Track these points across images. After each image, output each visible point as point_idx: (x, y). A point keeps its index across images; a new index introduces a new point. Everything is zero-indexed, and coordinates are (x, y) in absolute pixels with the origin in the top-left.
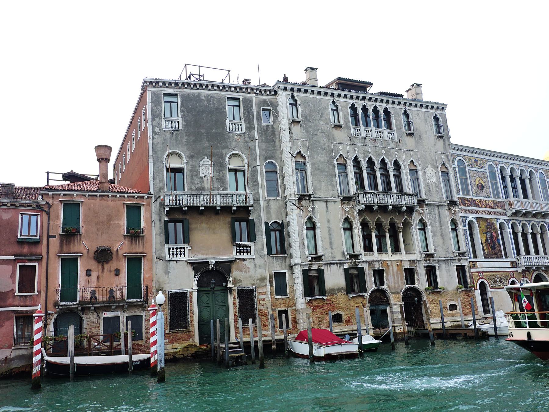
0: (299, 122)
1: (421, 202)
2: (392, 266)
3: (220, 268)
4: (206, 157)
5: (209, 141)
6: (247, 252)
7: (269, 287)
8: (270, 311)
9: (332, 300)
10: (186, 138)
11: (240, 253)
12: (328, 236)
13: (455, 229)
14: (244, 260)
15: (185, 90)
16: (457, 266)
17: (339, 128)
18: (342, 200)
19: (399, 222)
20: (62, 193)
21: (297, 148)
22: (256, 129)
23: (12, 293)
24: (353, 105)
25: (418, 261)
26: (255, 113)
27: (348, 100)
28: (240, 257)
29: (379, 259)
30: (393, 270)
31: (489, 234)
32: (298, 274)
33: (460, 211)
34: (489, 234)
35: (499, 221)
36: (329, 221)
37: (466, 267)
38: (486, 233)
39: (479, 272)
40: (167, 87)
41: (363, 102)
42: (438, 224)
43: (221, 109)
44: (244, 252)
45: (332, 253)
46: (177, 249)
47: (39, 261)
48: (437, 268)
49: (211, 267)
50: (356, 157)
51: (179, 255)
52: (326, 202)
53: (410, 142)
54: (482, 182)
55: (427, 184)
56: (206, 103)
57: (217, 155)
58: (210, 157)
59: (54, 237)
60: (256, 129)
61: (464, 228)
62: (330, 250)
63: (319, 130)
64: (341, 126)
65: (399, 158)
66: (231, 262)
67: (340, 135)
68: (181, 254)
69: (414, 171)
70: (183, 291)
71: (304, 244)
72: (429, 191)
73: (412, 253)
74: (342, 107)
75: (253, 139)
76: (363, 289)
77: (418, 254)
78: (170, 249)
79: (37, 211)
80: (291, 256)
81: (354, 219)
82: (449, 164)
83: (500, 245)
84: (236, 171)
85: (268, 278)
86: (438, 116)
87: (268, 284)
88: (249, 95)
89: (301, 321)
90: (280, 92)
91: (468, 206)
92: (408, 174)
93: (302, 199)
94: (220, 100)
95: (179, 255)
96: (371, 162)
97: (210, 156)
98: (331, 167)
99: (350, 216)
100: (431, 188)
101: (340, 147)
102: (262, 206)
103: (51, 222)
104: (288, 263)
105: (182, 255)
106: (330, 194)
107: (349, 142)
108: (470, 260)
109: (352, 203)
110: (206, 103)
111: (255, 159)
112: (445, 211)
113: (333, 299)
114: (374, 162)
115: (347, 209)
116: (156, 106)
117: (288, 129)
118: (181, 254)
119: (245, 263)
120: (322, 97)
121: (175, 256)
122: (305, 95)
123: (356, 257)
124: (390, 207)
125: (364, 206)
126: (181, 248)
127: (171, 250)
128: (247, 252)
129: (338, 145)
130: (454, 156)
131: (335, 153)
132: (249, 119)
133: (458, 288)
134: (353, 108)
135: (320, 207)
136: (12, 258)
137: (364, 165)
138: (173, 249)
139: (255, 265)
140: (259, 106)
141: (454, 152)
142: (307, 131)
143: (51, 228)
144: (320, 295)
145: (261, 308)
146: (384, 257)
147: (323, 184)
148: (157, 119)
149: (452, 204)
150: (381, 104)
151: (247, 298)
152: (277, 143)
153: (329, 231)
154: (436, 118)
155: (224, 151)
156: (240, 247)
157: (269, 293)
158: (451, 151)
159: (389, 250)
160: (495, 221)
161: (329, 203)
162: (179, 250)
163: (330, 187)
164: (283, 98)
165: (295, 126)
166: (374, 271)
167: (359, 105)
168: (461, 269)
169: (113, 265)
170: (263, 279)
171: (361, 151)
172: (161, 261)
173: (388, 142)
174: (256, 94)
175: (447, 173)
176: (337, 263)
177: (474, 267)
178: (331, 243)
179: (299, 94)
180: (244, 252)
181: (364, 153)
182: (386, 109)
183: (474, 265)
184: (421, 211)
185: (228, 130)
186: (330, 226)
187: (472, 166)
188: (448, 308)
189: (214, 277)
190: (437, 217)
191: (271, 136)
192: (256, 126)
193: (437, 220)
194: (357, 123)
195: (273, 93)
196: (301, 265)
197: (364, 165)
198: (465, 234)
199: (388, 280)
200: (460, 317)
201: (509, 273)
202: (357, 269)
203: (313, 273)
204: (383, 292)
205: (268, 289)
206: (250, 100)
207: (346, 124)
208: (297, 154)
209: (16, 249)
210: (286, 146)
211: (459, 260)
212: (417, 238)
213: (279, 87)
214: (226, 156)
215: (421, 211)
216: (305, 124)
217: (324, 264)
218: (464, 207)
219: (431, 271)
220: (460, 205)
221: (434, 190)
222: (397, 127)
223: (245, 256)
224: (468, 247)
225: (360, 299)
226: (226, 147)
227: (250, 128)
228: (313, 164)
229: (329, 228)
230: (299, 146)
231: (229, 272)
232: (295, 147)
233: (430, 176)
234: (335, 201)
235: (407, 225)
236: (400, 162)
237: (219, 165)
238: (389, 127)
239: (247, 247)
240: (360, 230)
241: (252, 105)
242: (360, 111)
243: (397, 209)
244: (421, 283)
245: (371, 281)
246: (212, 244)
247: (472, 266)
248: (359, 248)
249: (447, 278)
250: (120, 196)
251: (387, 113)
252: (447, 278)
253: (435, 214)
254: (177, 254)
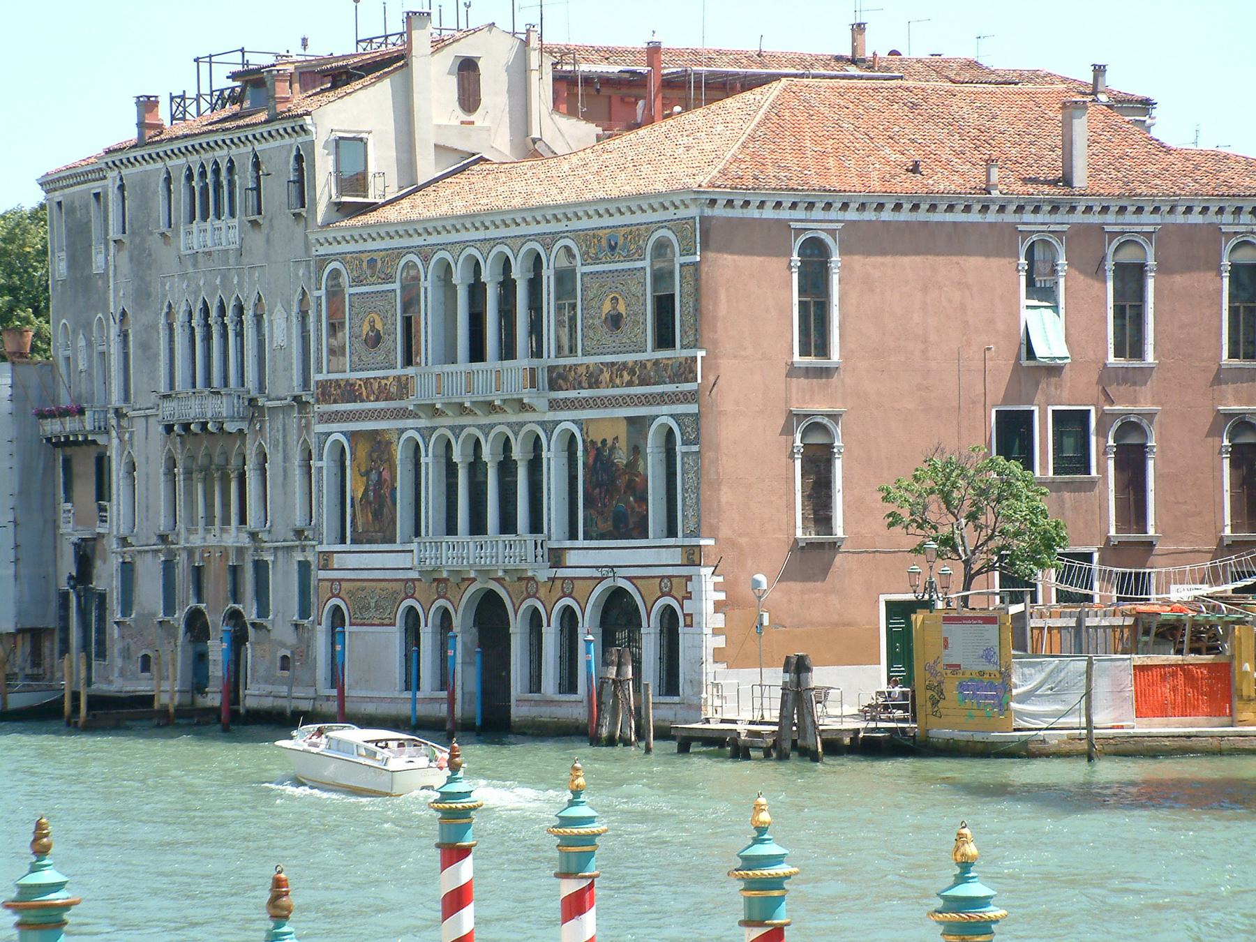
31: (374, 476)
34: (374, 476)
35: (405, 436)
38: (367, 473)
39: (332, 581)
42: (280, 455)
54: (379, 326)
66: (94, 539)
83: (395, 504)
91: (335, 402)
131: (162, 303)
135: (139, 426)
160: (394, 438)
183: (326, 560)
187: (358, 281)
188: (279, 664)
194: (193, 218)
200: (285, 689)
201: (402, 584)
211: (303, 549)
218: (325, 408)
220: (318, 401)
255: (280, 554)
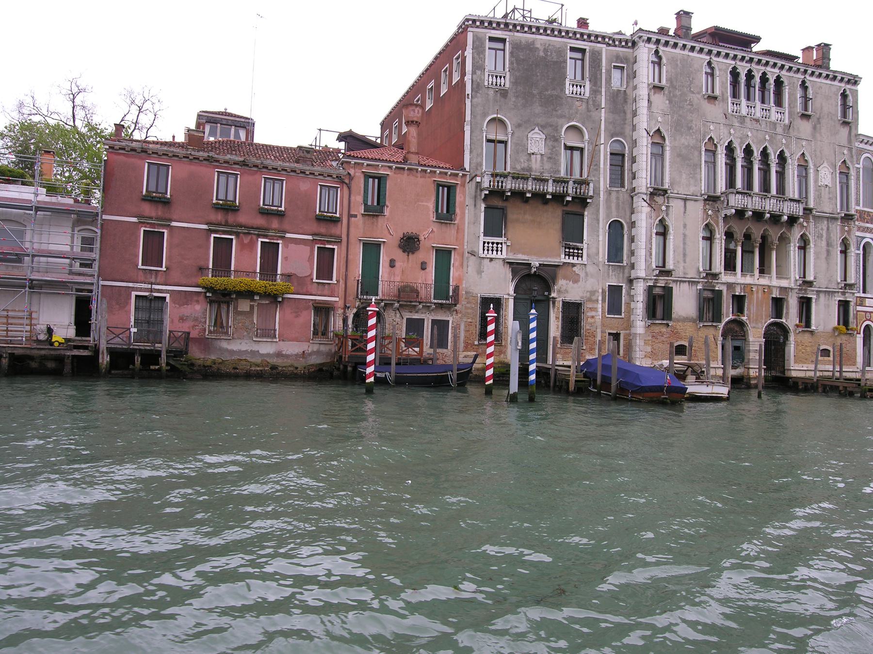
0: (662, 88)
1: (808, 211)
2: (757, 292)
3: (543, 274)
4: (537, 130)
5: (541, 106)
6: (578, 256)
7: (600, 302)
8: (599, 330)
9: (678, 327)
10: (513, 99)
11: (569, 256)
12: (682, 245)
13: (844, 252)
14: (573, 265)
15: (516, 34)
16: (839, 301)
17: (712, 101)
18: (705, 200)
19: (774, 234)
20: (366, 163)
21: (655, 124)
22: (603, 93)
23: (309, 279)
24: (735, 68)
25: (792, 289)
26: (604, 71)
27: (729, 61)
28: (568, 261)
29: (742, 282)
30: (757, 297)
32: (640, 290)
33: (856, 229)
36: (685, 226)
37: (852, 304)
39: (866, 312)
40: (494, 29)
41: (748, 65)
42: (824, 243)
43: (561, 62)
44: (573, 256)
45: (684, 268)
46: (493, 243)
47: (339, 242)
48: (814, 301)
49: (534, 270)
50: (730, 143)
51: (495, 252)
52: (685, 200)
53: (805, 127)
55: (818, 188)
56: (542, 54)
57: (551, 126)
58: (542, 127)
59: (356, 216)
60: (603, 93)
61: (858, 252)
62: (682, 264)
63: (686, 101)
64: (715, 98)
65: (787, 147)
67: (713, 111)
68: (497, 251)
69: (803, 167)
70: (497, 296)
71: (651, 254)
72: (819, 197)
73: (783, 279)
74: (720, 70)
75: (598, 107)
76: (717, 317)
77: (793, 279)
78: (484, 243)
79: (337, 182)
80: (632, 266)
81: (718, 226)
82: (852, 162)
84: (572, 149)
85: (600, 291)
86: (848, 92)
87: (600, 298)
88: (599, 45)
89: (638, 349)
90: (641, 44)
92: (796, 172)
93: (655, 194)
94: (560, 52)
95: (495, 252)
96: (748, 151)
97: (542, 126)
98: (696, 153)
99: (712, 222)
100: (823, 194)
101: (712, 127)
102: (601, 199)
103: (352, 198)
104: (626, 275)
105: (499, 253)
106: (692, 189)
107: (723, 121)
108: (858, 295)
109: (718, 205)
110: (542, 54)
111: (599, 135)
112: (836, 227)
113: (679, 326)
114: (752, 151)
115: (710, 212)
116: (478, 54)
117: (646, 97)
118: (497, 251)
119: (575, 269)
120: (695, 54)
121: (490, 252)
122: (673, 50)
123: (715, 276)
124: (768, 215)
125: (733, 211)
126: (497, 244)
127: (486, 245)
128: (578, 256)
129: (708, 124)
130: (861, 151)
131: (704, 136)
132: (595, 80)
133: (835, 329)
134: (735, 74)
135: (676, 206)
136: (310, 237)
137: (739, 154)
138: (488, 243)
139: (586, 273)
140: (609, 62)
141: (862, 146)
142: (670, 102)
143: (352, 205)
144: (663, 319)
145: (588, 327)
146: (748, 280)
147: (684, 176)
148: (478, 72)
149: (848, 218)
150: (773, 70)
151: (573, 314)
152: (629, 116)
153: (684, 239)
154: (844, 96)
155: (561, 121)
156: (569, 248)
157: (600, 310)
158: (857, 144)
159: (757, 272)
161: (688, 203)
162: (495, 245)
163: (692, 181)
164: (644, 53)
165: (657, 95)
166: (734, 296)
167: (743, 69)
168: (844, 305)
169: (420, 256)
170: (593, 293)
171: (738, 134)
172: (473, 257)
173: (774, 124)
174: (608, 45)
175: (847, 175)
176: (689, 282)
177: (861, 305)
178: (685, 255)
179: (665, 49)
180: (573, 256)
181: (741, 138)
182: (778, 77)
183: (861, 302)
184: (805, 224)
185: (567, 92)
186: (687, 233)
189: (534, 284)
190: (825, 235)
191: (621, 103)
192: (603, 90)
193: (824, 238)
195: (630, 44)
196: (644, 279)
197: (739, 154)
198: (857, 260)
199: (749, 309)
202: (713, 291)
203: (657, 291)
204: (741, 324)
205: (600, 306)
206: (599, 53)
207: (723, 95)
208: (655, 132)
209: (315, 227)
210: (643, 121)
211: (844, 293)
212: (795, 259)
213: (640, 37)
214: (562, 128)
215: (805, 224)
216: (670, 92)
217: (674, 281)
219: (805, 304)
221: (827, 196)
222: (789, 105)
223: (575, 261)
224: (857, 278)
225: (712, 329)
226: (562, 116)
227: (595, 91)
228: (673, 149)
229: (685, 235)
230: (660, 122)
231: (554, 279)
232: (654, 122)
233: (825, 176)
234: (696, 201)
235: (784, 239)
236: (787, 154)
237: (553, 138)
238: (779, 103)
239: (578, 249)
240: (723, 241)
241: (601, 60)
242: (743, 78)
243: (775, 218)
244: (791, 319)
245: (728, 308)
246: (535, 240)
247: (859, 302)
248: (719, 265)
249: (825, 316)
250: (431, 171)
251: (779, 82)
252: (825, 316)
253: (822, 229)
254: (492, 250)
255: (822, 295)
